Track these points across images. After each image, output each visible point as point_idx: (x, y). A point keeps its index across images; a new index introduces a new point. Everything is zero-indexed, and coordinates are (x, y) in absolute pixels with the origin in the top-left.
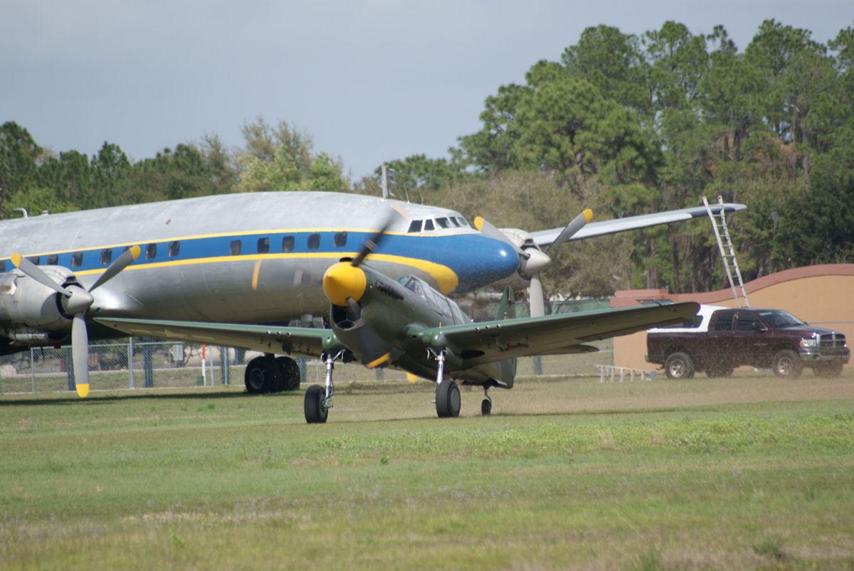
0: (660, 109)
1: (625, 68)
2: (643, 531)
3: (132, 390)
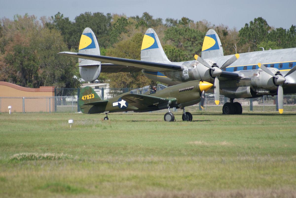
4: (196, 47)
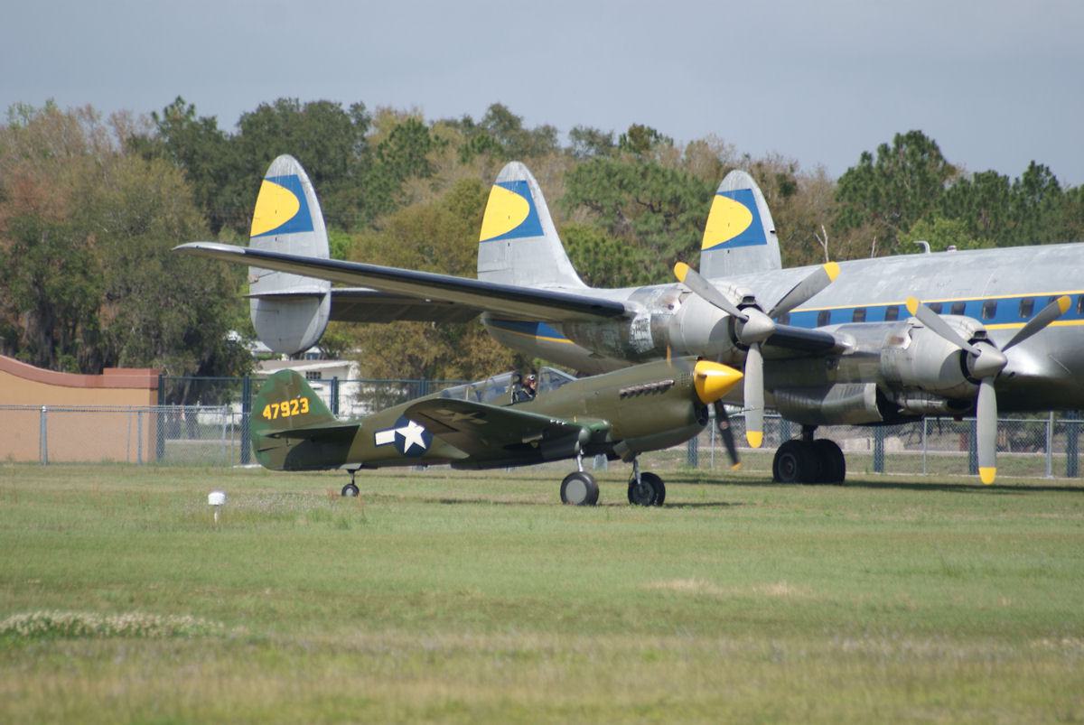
3: (1049, 479)
4: (678, 234)
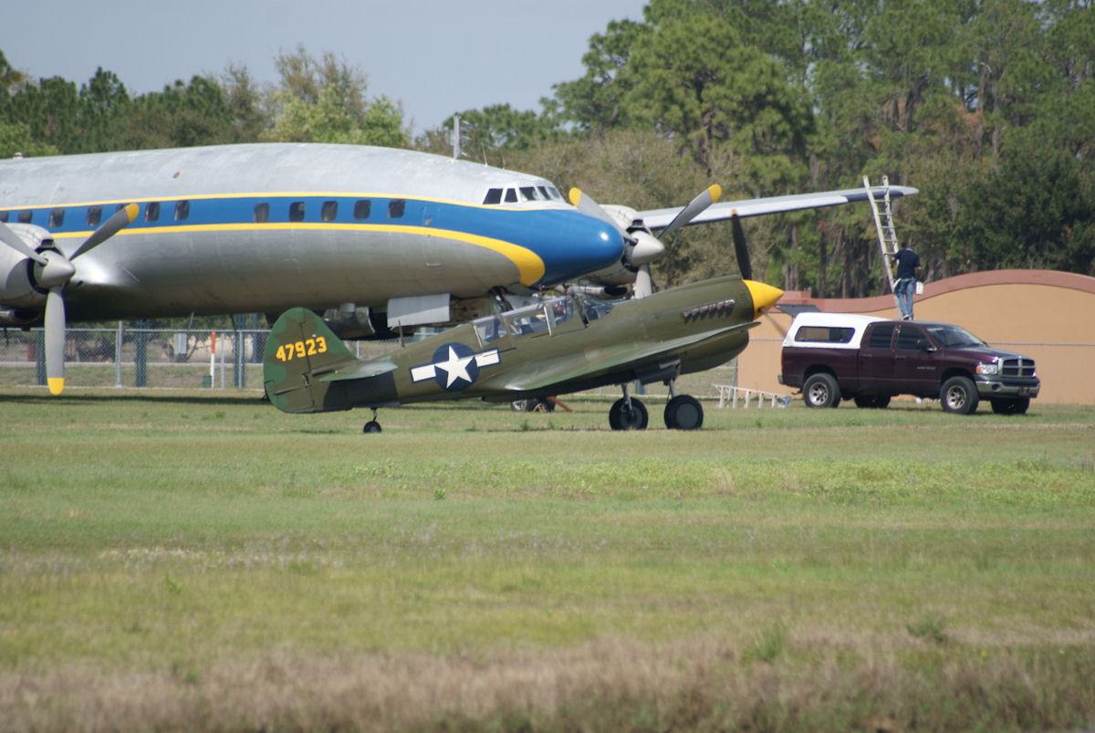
0: (813, 61)
1: (771, 6)
2: (768, 600)
3: (118, 388)
